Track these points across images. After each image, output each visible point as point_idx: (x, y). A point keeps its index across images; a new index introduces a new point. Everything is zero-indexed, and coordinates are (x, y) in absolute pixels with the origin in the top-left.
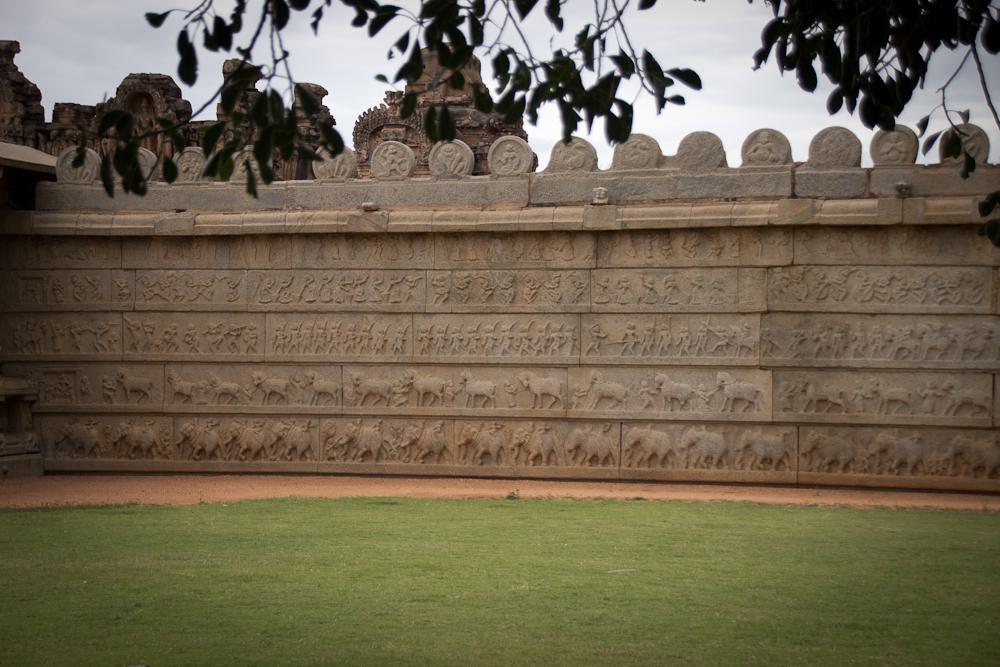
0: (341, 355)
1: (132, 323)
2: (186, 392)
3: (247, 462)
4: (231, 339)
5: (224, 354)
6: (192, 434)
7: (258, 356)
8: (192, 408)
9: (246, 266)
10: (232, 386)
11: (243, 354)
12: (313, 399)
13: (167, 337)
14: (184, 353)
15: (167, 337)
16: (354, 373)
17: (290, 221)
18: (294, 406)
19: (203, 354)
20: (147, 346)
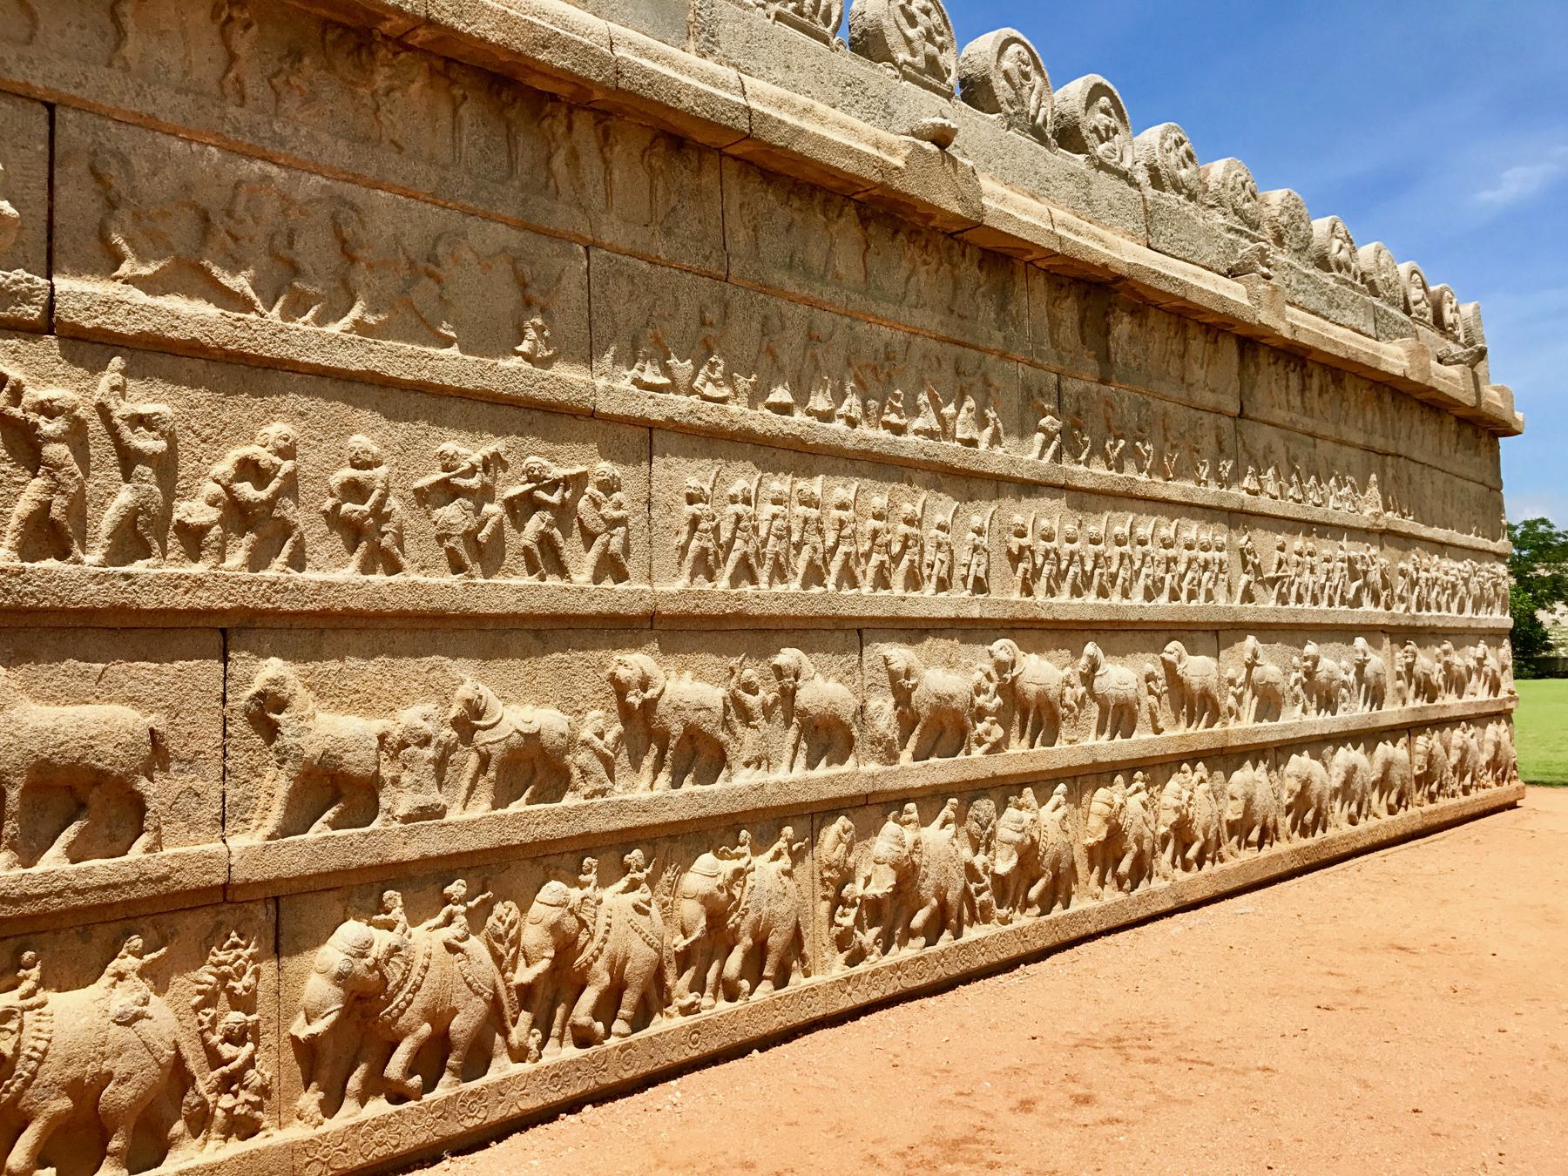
0: (864, 599)
1: (36, 393)
2: (358, 761)
3: (613, 1041)
4: (535, 524)
5: (513, 589)
6: (394, 973)
7: (629, 594)
8: (388, 837)
9: (584, 229)
10: (548, 720)
11: (579, 585)
12: (796, 747)
13: (247, 490)
14: (336, 575)
15: (247, 490)
16: (899, 654)
17: (756, 96)
18: (740, 783)
19: (426, 581)
20: (133, 539)
